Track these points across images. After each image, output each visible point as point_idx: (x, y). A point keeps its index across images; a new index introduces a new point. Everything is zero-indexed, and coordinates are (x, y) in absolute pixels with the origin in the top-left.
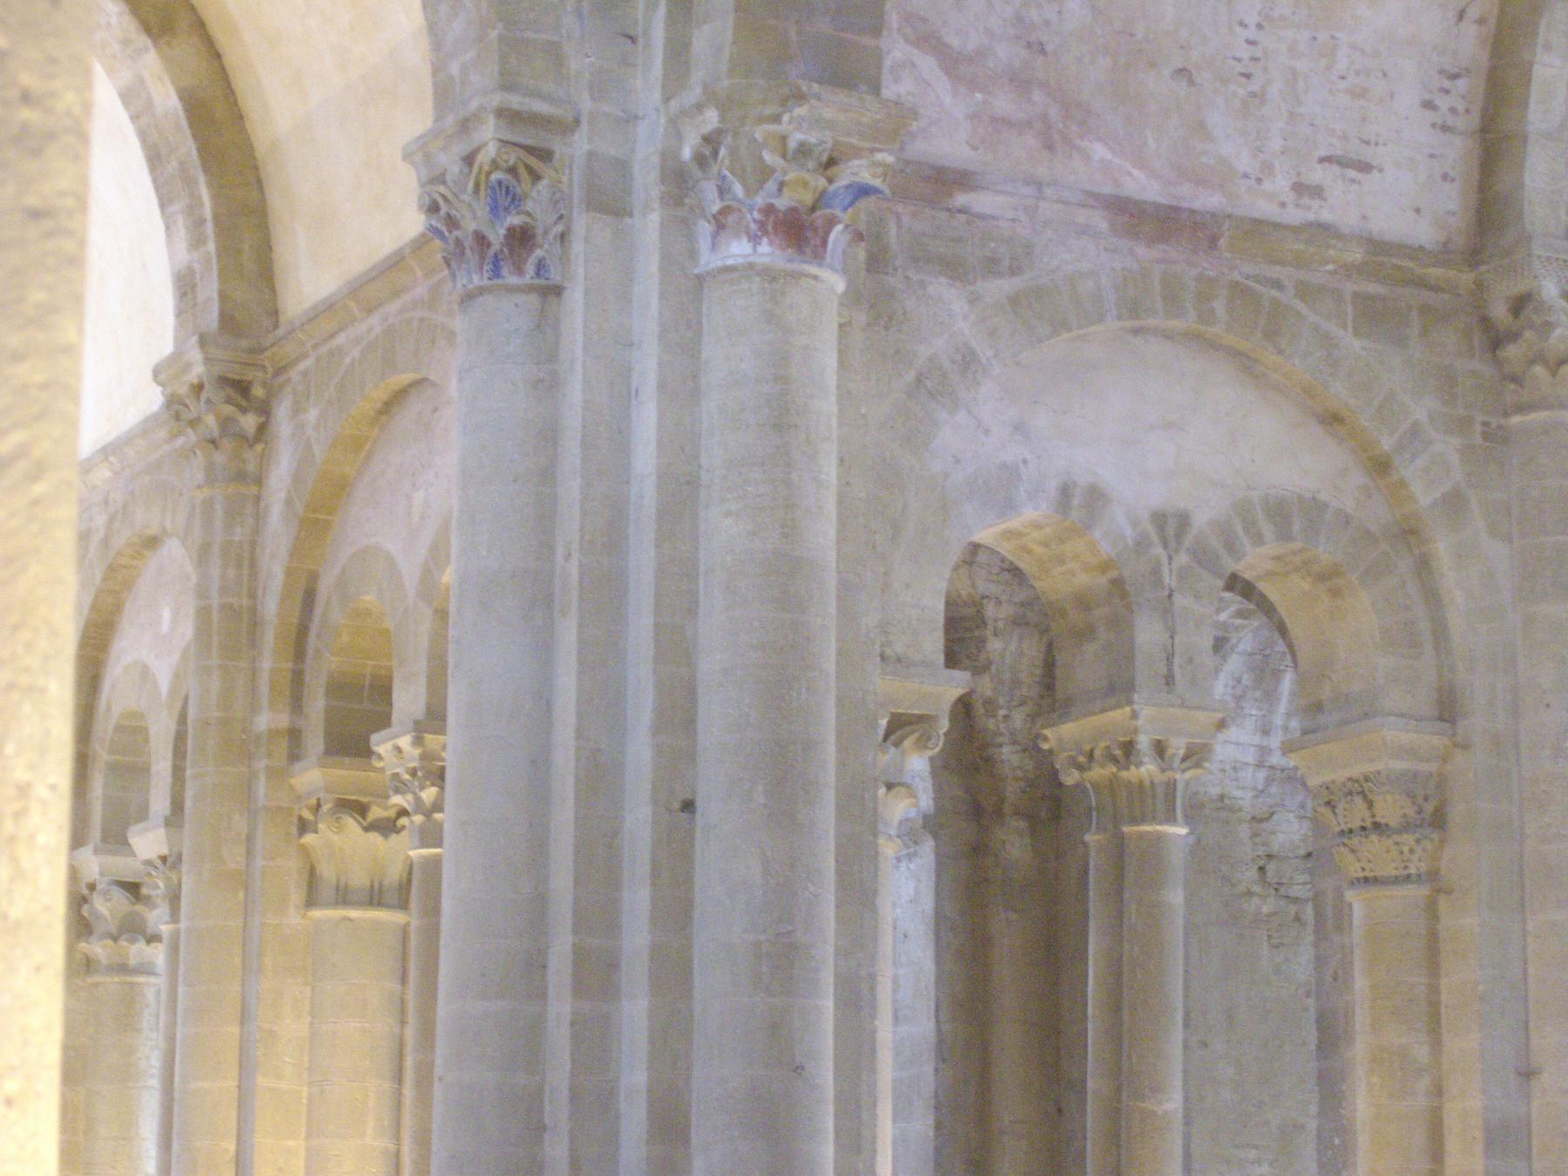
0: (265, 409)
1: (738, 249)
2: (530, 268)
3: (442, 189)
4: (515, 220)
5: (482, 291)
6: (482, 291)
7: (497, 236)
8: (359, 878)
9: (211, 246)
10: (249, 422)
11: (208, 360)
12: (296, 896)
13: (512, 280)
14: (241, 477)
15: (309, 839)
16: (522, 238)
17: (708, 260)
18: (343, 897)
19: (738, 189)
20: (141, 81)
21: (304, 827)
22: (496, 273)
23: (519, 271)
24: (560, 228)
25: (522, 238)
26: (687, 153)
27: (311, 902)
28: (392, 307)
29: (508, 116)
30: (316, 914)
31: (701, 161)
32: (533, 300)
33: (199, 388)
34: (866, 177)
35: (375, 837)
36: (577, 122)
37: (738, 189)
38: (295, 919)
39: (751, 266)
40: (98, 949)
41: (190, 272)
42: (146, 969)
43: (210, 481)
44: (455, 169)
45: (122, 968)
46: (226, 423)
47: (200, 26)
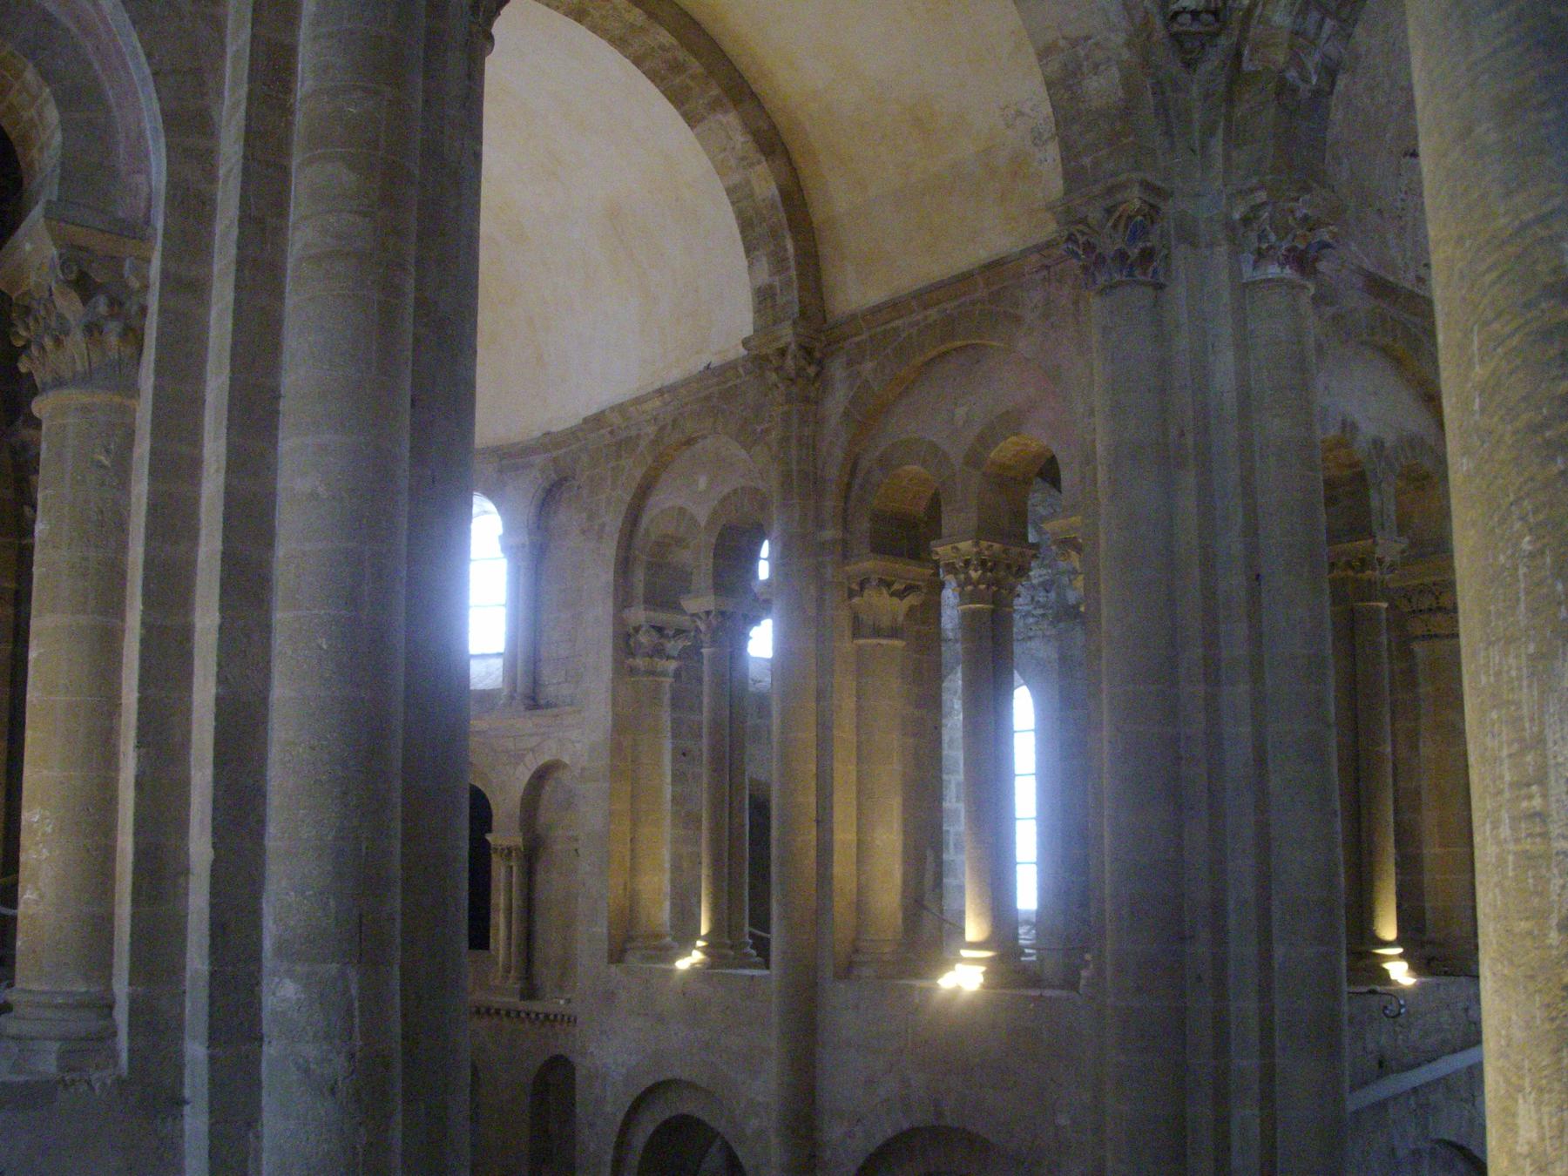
0: (820, 363)
1: (1273, 270)
2: (1151, 270)
3: (1081, 227)
5: (1120, 284)
6: (1120, 284)
7: (1134, 252)
8: (886, 622)
9: (793, 273)
10: (812, 371)
11: (797, 335)
12: (848, 633)
13: (1141, 278)
14: (807, 400)
15: (856, 600)
16: (1147, 255)
17: (1248, 273)
18: (877, 632)
19: (1273, 238)
20: (748, 182)
22: (1130, 275)
23: (1145, 274)
24: (1165, 252)
25: (1147, 255)
26: (1237, 216)
27: (855, 635)
28: (950, 306)
29: (1147, 186)
30: (861, 641)
31: (1246, 221)
32: (1150, 291)
33: (782, 353)
34: (1327, 238)
35: (895, 600)
36: (1172, 194)
37: (1273, 238)
38: (848, 646)
39: (1282, 280)
40: (640, 662)
41: (771, 287)
42: (664, 674)
43: (789, 401)
44: (1095, 215)
45: (653, 673)
46: (800, 371)
47: (786, 152)
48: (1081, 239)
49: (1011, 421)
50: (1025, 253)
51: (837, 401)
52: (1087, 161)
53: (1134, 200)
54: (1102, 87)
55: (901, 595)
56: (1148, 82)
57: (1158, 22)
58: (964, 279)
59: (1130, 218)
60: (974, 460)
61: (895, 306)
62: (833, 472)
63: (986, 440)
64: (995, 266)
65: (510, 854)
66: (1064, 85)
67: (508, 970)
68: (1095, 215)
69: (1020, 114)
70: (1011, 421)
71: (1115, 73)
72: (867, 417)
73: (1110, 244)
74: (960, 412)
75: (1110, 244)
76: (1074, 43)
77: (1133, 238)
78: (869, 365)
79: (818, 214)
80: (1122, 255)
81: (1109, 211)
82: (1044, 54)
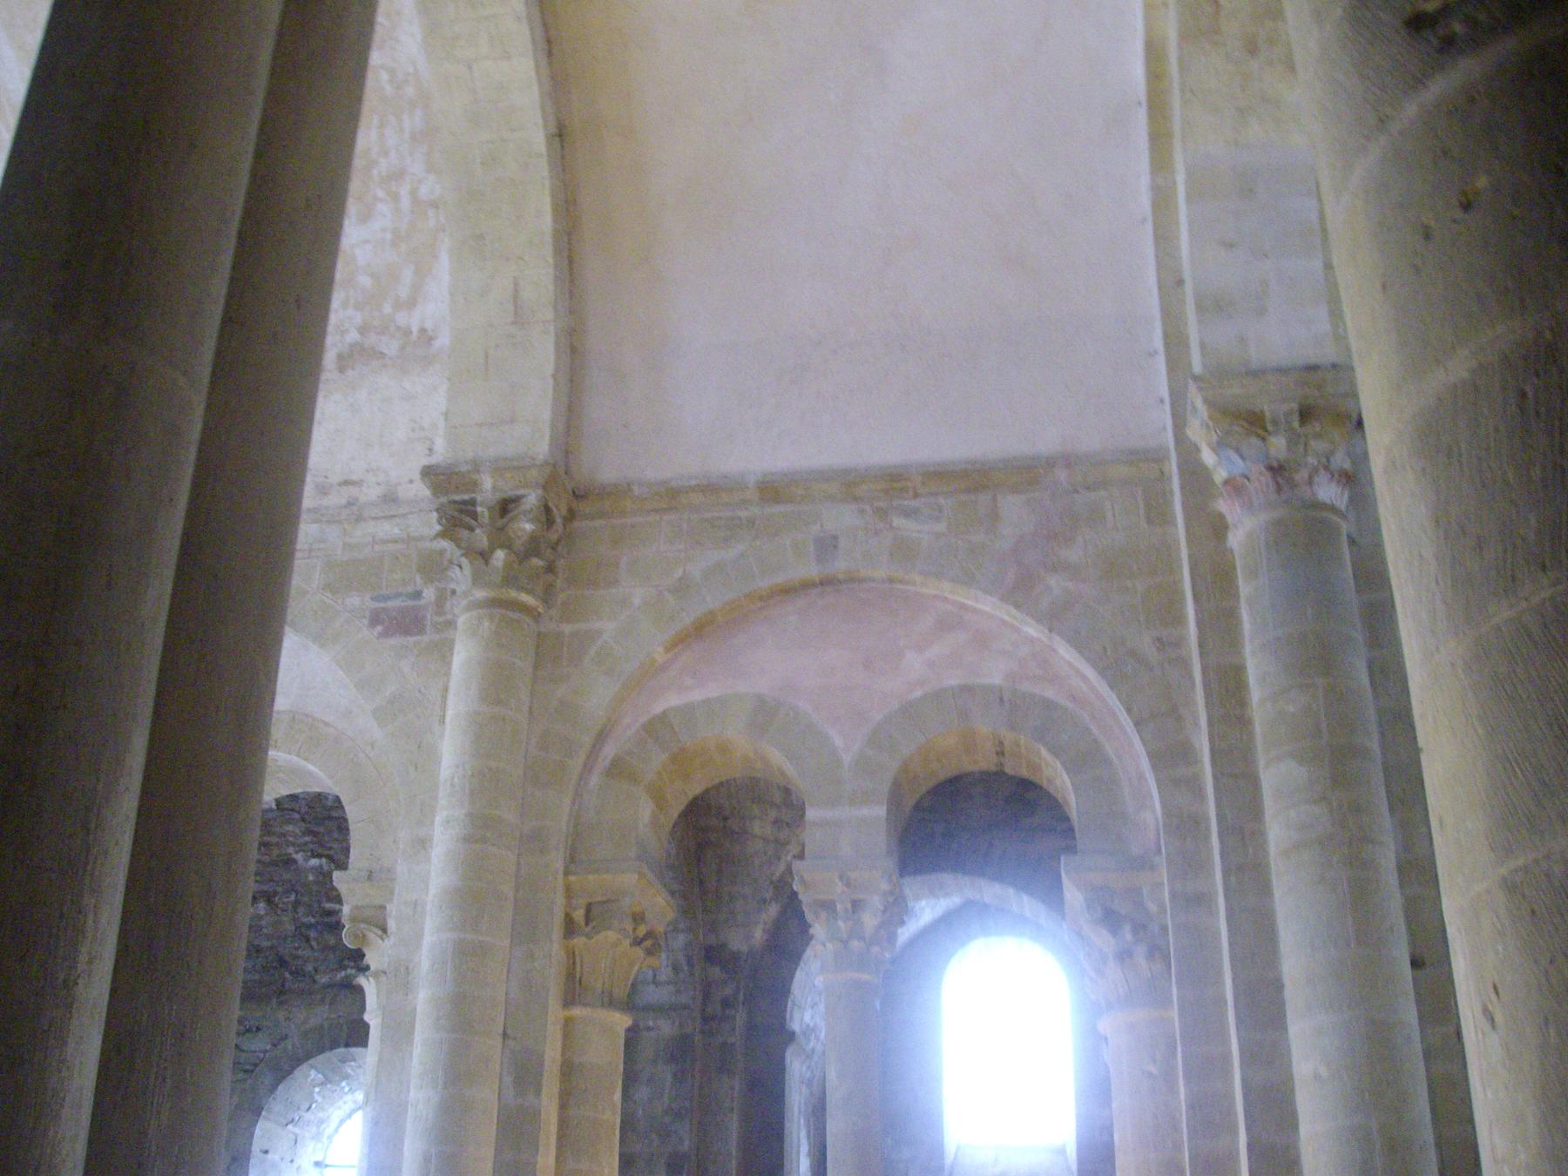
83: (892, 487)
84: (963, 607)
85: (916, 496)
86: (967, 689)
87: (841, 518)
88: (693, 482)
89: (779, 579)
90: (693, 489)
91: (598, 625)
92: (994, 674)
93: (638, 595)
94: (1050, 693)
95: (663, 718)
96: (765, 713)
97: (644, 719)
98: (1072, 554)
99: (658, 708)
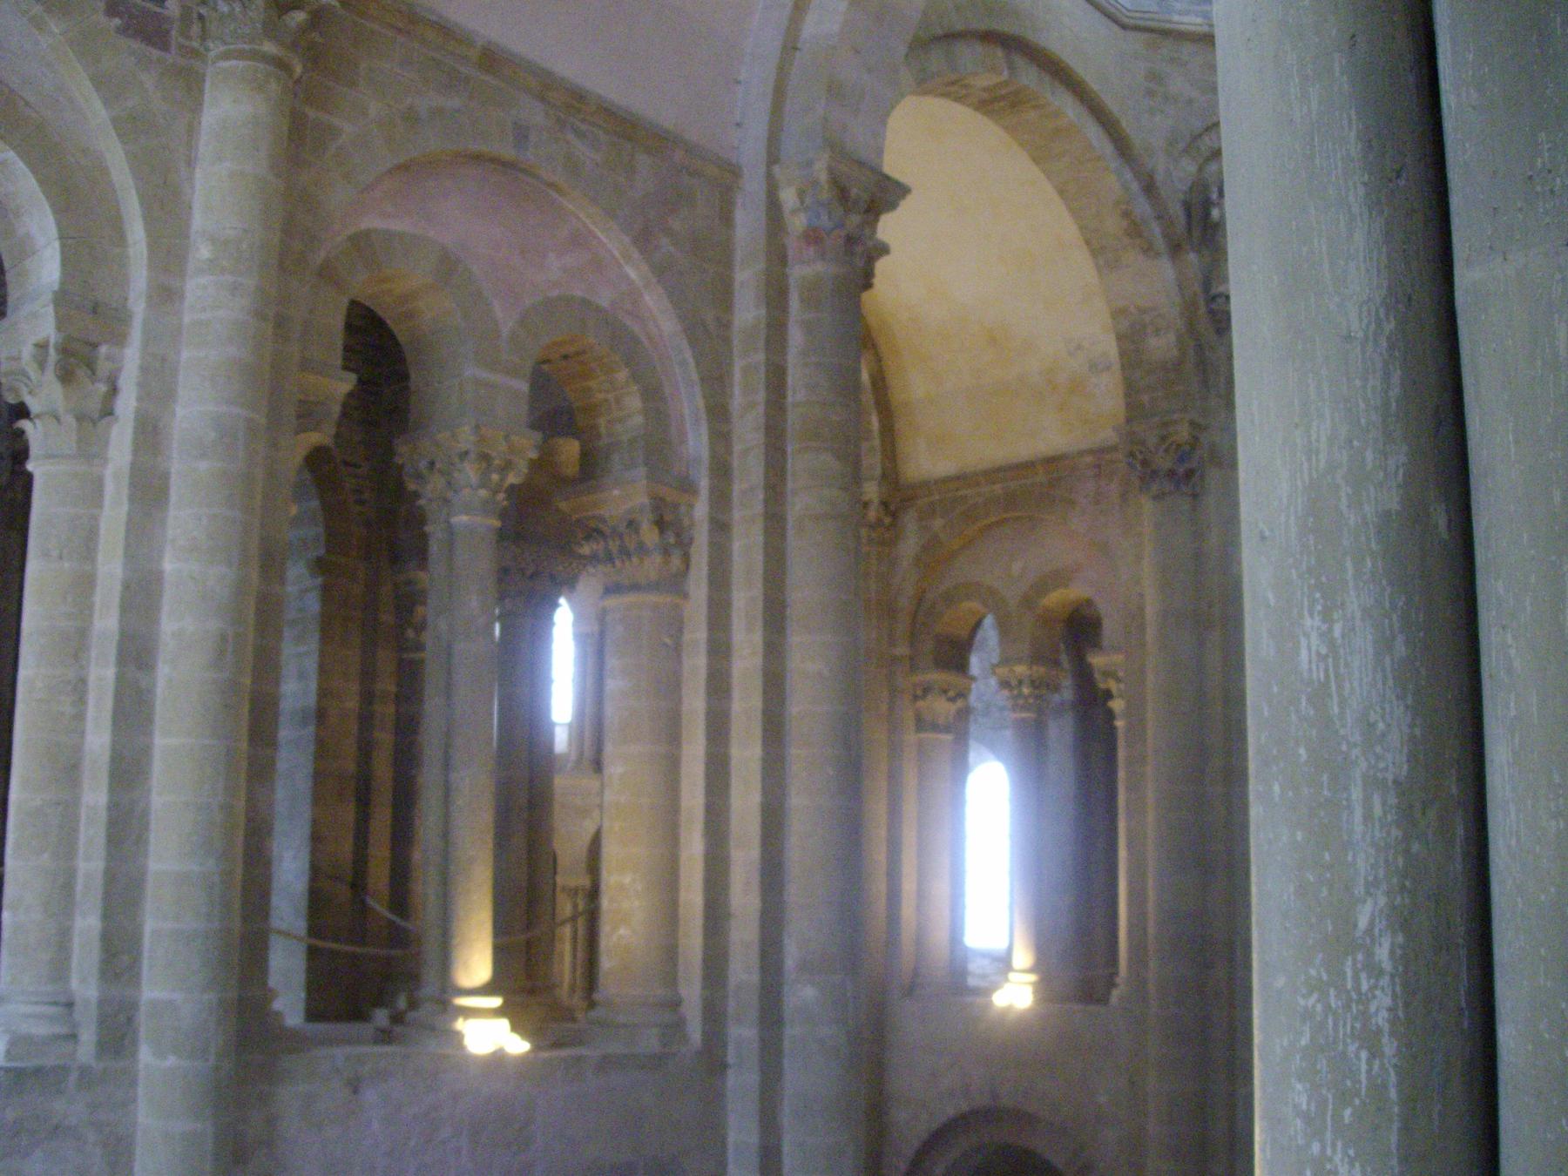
0: (894, 515)
4: (1187, 466)
10: (887, 520)
13: (1184, 489)
15: (920, 703)
16: (1189, 474)
21: (916, 698)
25: (1189, 474)
29: (1192, 423)
30: (922, 735)
38: (911, 737)
44: (1152, 441)
46: (879, 522)
48: (1140, 457)
49: (1059, 578)
50: (1082, 453)
51: (910, 544)
52: (1145, 398)
53: (1183, 433)
54: (1162, 345)
55: (952, 700)
56: (1192, 343)
57: (1202, 303)
58: (1028, 466)
59: (1179, 446)
60: (1028, 602)
61: (961, 478)
62: (905, 603)
63: (1041, 588)
64: (1051, 461)
65: (576, 893)
66: (1131, 339)
67: (573, 990)
68: (1152, 441)
69: (1079, 347)
70: (1059, 578)
71: (1172, 337)
72: (933, 558)
73: (1164, 462)
74: (1016, 567)
75: (1164, 462)
76: (1142, 311)
77: (1181, 460)
78: (938, 523)
79: (897, 396)
80: (1171, 474)
81: (1163, 438)
82: (1118, 313)
83: (573, 105)
84: (590, 232)
85: (583, 121)
86: (585, 302)
87: (534, 114)
88: (434, 18)
89: (484, 148)
90: (432, 24)
91: (336, 121)
92: (604, 299)
93: (374, 108)
94: (636, 329)
95: (367, 234)
96: (448, 266)
97: (352, 230)
98: (676, 224)
99: (363, 227)
